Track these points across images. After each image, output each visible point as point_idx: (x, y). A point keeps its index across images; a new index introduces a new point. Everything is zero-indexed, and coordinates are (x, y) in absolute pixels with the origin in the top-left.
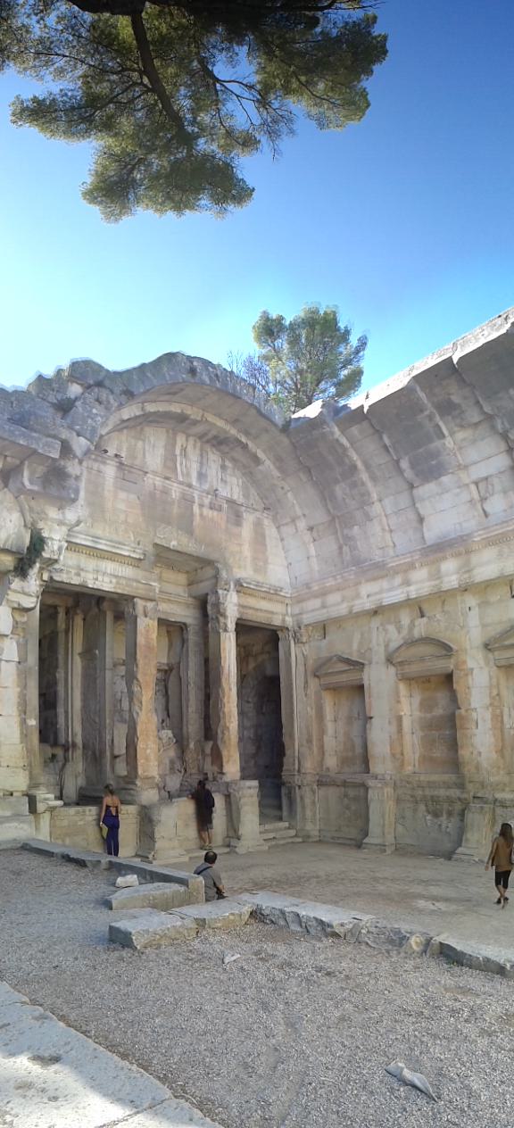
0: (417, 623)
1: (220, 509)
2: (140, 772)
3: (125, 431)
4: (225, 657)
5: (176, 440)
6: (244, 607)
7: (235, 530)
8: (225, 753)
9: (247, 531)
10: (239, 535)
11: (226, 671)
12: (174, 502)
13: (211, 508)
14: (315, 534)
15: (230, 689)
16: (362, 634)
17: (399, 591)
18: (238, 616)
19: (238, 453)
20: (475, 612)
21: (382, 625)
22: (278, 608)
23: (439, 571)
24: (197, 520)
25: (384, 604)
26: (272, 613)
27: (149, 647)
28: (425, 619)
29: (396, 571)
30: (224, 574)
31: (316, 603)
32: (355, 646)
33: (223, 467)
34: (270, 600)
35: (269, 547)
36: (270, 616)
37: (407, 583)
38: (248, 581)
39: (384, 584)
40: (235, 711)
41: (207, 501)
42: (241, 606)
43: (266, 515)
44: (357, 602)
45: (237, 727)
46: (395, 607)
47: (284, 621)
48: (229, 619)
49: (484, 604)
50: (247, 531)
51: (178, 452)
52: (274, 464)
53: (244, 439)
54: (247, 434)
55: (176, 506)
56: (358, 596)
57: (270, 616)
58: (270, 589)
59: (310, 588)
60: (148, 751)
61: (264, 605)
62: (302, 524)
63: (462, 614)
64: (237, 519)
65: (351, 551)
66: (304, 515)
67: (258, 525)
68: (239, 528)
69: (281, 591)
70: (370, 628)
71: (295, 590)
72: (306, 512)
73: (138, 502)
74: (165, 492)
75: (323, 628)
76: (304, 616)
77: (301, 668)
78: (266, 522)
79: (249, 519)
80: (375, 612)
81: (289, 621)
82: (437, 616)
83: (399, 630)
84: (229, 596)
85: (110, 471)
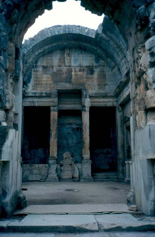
2: (50, 155)
3: (45, 56)
4: (84, 120)
5: (65, 52)
6: (92, 102)
7: (90, 76)
9: (95, 75)
10: (92, 78)
11: (84, 124)
12: (64, 73)
13: (80, 71)
15: (86, 130)
18: (90, 106)
22: (111, 100)
24: (73, 77)
26: (107, 102)
27: (54, 119)
30: (84, 93)
36: (106, 103)
38: (92, 93)
41: (78, 69)
45: (89, 143)
47: (113, 104)
48: (86, 107)
50: (95, 75)
51: (65, 55)
55: (65, 74)
57: (106, 103)
60: (54, 149)
68: (92, 75)
69: (108, 94)
73: (50, 76)
74: (60, 71)
79: (97, 71)
84: (86, 100)
85: (40, 69)
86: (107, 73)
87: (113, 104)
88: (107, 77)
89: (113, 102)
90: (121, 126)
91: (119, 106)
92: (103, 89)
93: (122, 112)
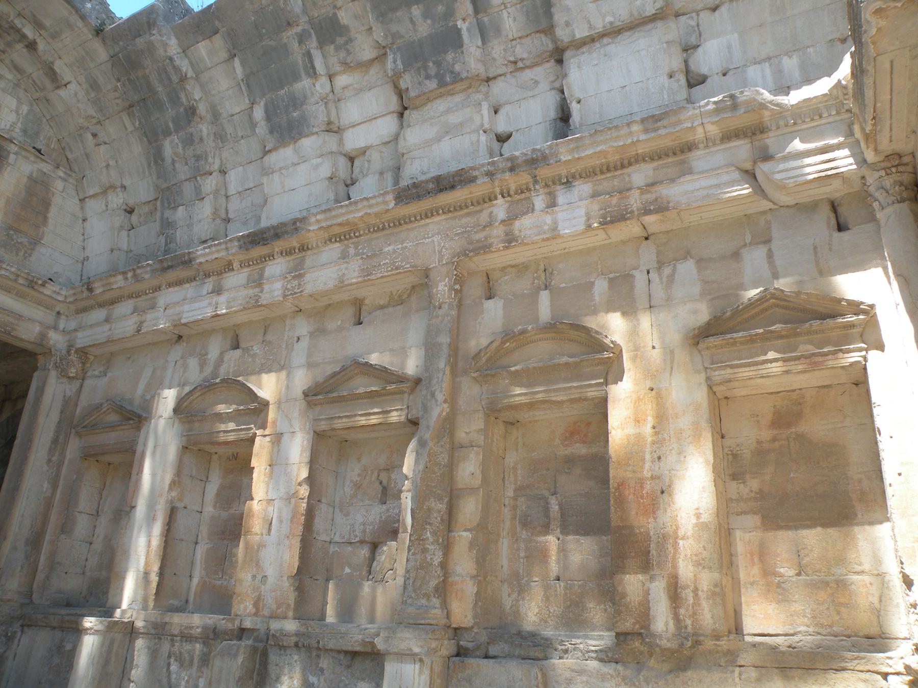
0: (227, 357)
14: (134, 218)
16: (154, 372)
20: (304, 344)
21: (182, 358)
22: (39, 314)
23: (261, 276)
25: (184, 321)
28: (238, 352)
31: (99, 315)
34: (21, 295)
35: (51, 221)
36: (11, 319)
37: (218, 291)
39: (189, 290)
43: (61, 174)
44: (150, 316)
47: (43, 336)
49: (319, 332)
52: (87, 93)
58: (18, 276)
59: (90, 290)
62: (117, 200)
63: (287, 345)
65: (166, 244)
66: (124, 187)
70: (167, 361)
71: (72, 292)
72: (127, 183)
76: (80, 334)
77: (55, 417)
78: (59, 185)
81: (56, 339)
82: (255, 348)
83: (202, 365)
86: (57, 200)
87: (43, 336)
88: (53, 212)
89: (48, 328)
90: (55, 441)
91: (73, 357)
92: (21, 253)
93: (76, 385)
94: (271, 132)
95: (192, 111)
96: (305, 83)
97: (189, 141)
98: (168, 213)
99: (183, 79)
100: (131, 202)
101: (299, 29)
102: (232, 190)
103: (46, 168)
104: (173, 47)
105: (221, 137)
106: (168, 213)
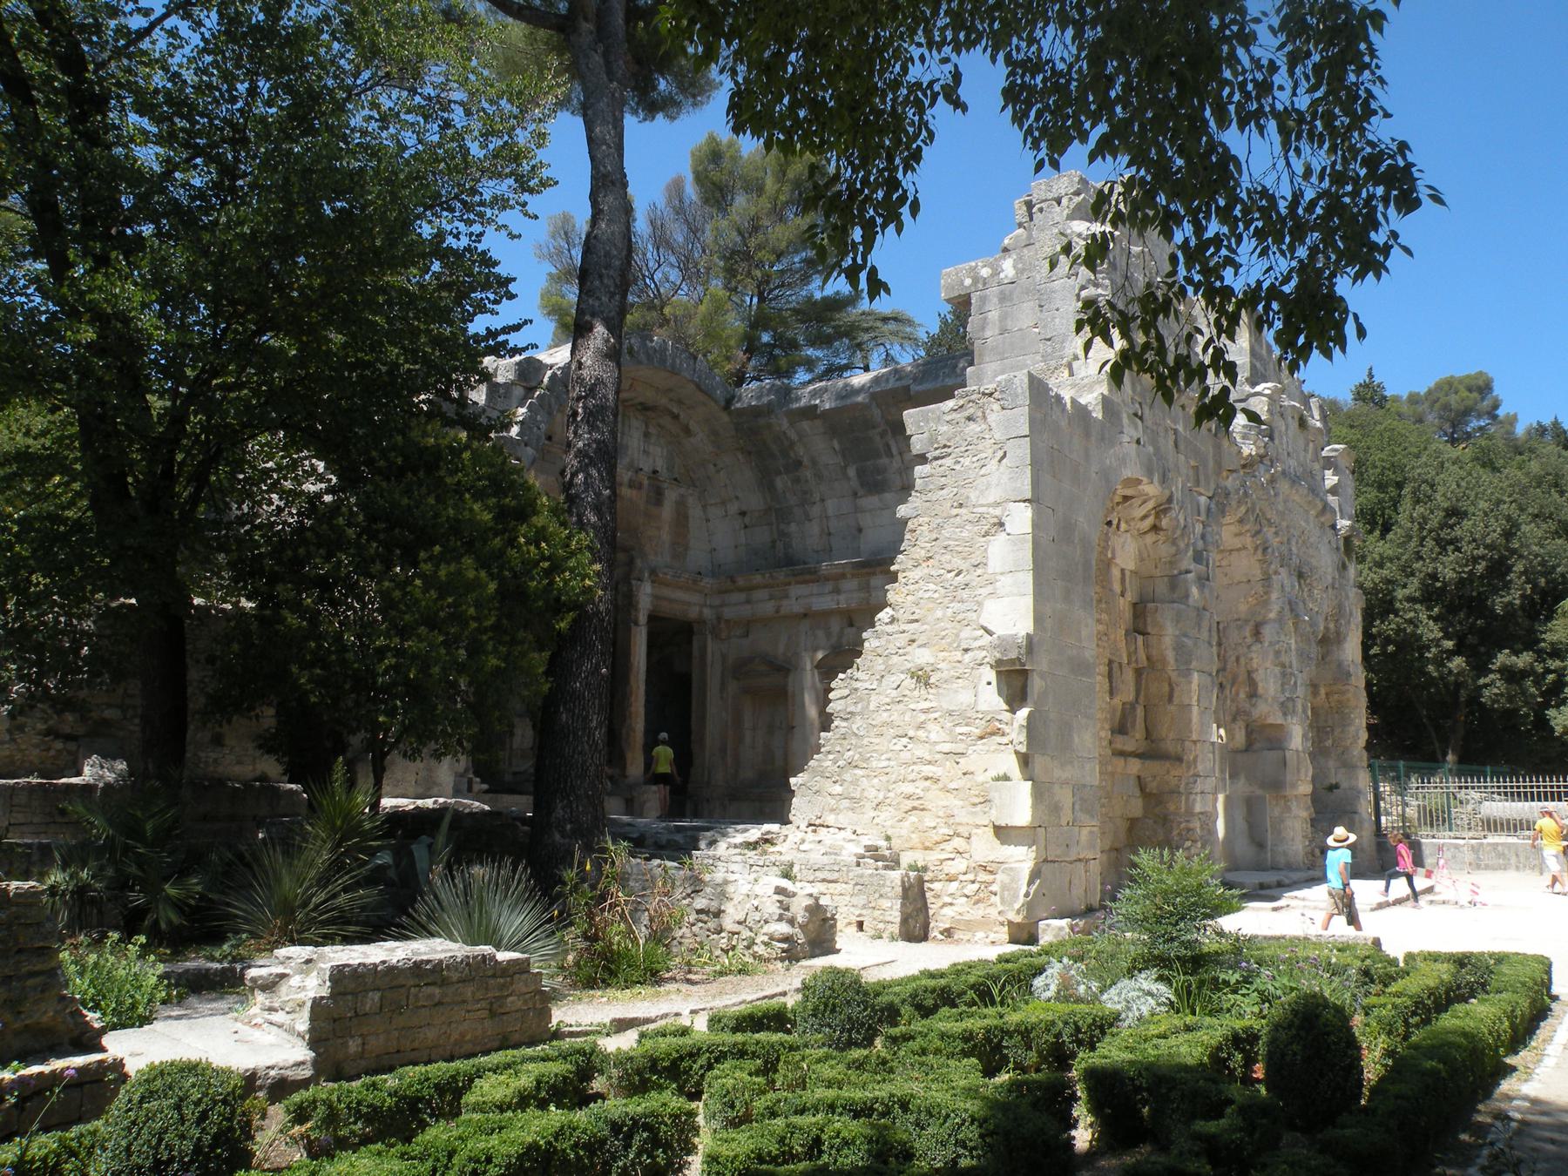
1: (640, 487)
8: (629, 755)
13: (630, 486)
14: (747, 520)
17: (829, 598)
19: (666, 421)
22: (695, 598)
26: (689, 604)
29: (827, 579)
30: (639, 563)
31: (742, 596)
32: (781, 649)
33: (647, 435)
37: (837, 591)
39: (814, 588)
40: (642, 711)
42: (656, 597)
44: (785, 602)
46: (827, 614)
47: (701, 613)
50: (667, 511)
53: (675, 411)
54: (680, 402)
56: (787, 597)
61: (679, 595)
62: (733, 508)
64: (657, 496)
67: (681, 504)
75: (748, 626)
78: (690, 500)
80: (805, 615)
87: (701, 613)
94: (862, 485)
95: (798, 464)
96: (884, 461)
97: (797, 480)
98: (782, 526)
99: (792, 444)
100: (744, 508)
101: (880, 430)
102: (830, 513)
103: (682, 491)
104: (785, 424)
105: (819, 477)
106: (782, 526)
